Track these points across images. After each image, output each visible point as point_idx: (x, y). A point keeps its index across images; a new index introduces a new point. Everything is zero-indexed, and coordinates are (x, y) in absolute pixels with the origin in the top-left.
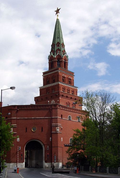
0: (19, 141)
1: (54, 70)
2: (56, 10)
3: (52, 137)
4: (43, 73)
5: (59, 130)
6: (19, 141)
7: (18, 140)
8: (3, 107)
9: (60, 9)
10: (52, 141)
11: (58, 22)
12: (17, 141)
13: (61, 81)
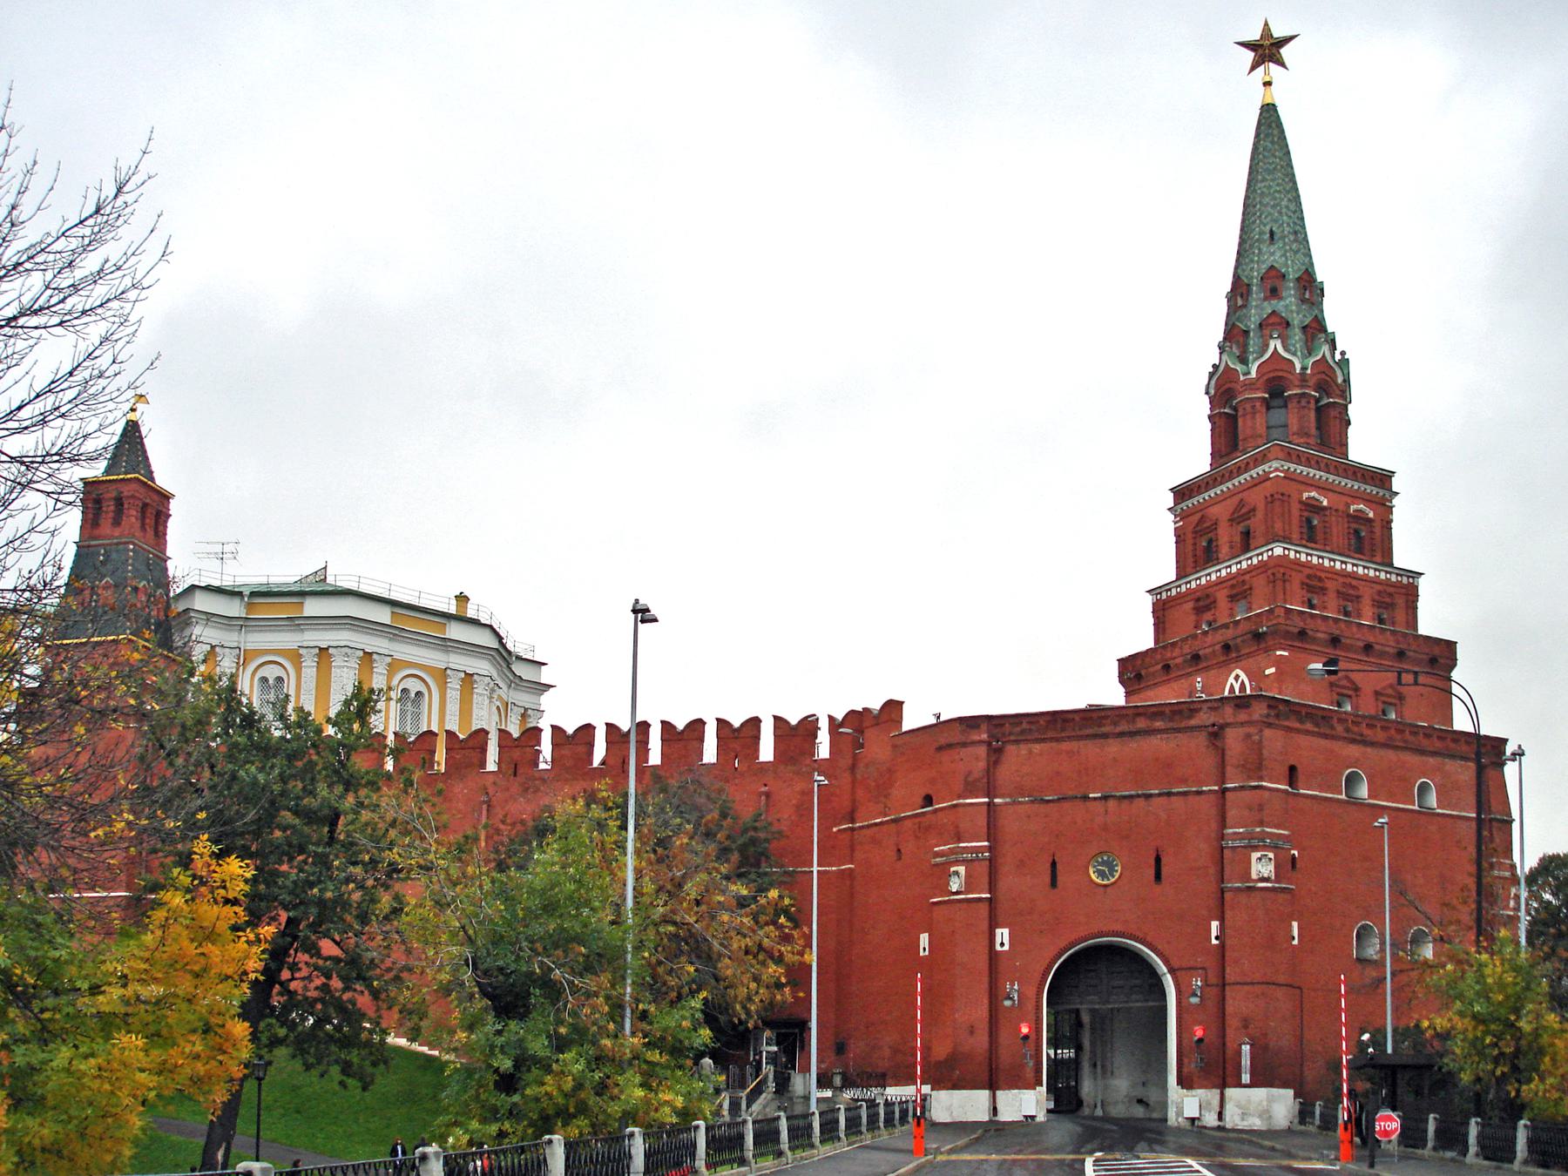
0: (1006, 947)
1: (1247, 467)
3: (1228, 914)
4: (1171, 495)
5: (1272, 867)
7: (1002, 944)
10: (1228, 942)
11: (1269, 118)
12: (998, 948)
13: (1295, 536)
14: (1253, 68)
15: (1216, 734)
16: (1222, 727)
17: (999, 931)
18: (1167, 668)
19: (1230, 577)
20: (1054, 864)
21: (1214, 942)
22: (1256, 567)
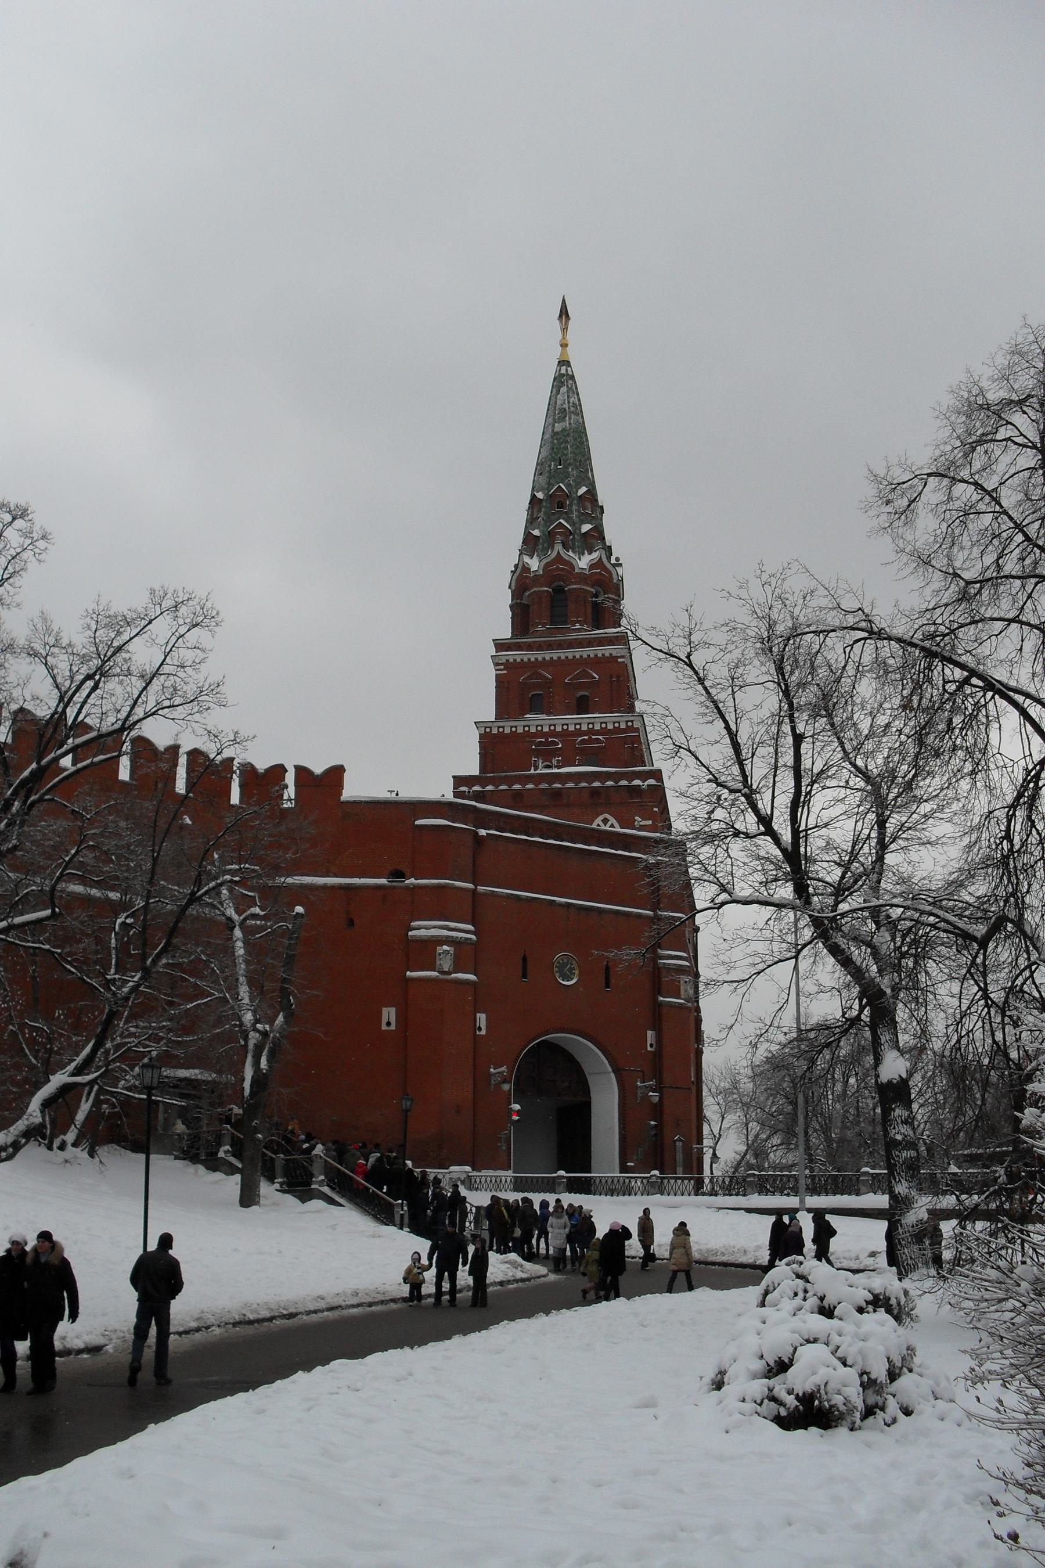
6: (483, 1032)
8: (348, 802)
11: (564, 379)
17: (478, 1015)
21: (649, 1049)
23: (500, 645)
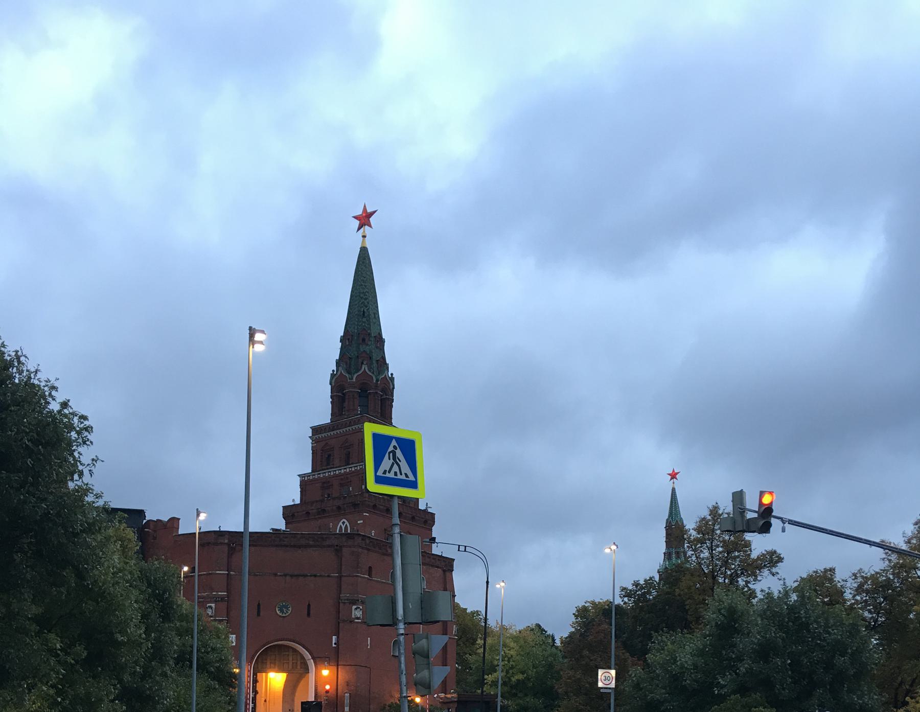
2: (359, 212)
3: (341, 634)
9: (375, 212)
14: (359, 229)
15: (338, 550)
16: (341, 547)
18: (308, 513)
19: (340, 475)
20: (259, 605)
22: (353, 472)
23: (316, 430)
